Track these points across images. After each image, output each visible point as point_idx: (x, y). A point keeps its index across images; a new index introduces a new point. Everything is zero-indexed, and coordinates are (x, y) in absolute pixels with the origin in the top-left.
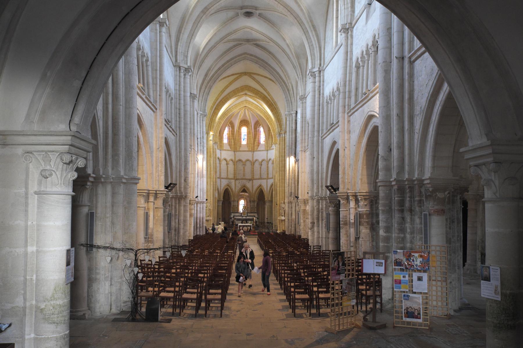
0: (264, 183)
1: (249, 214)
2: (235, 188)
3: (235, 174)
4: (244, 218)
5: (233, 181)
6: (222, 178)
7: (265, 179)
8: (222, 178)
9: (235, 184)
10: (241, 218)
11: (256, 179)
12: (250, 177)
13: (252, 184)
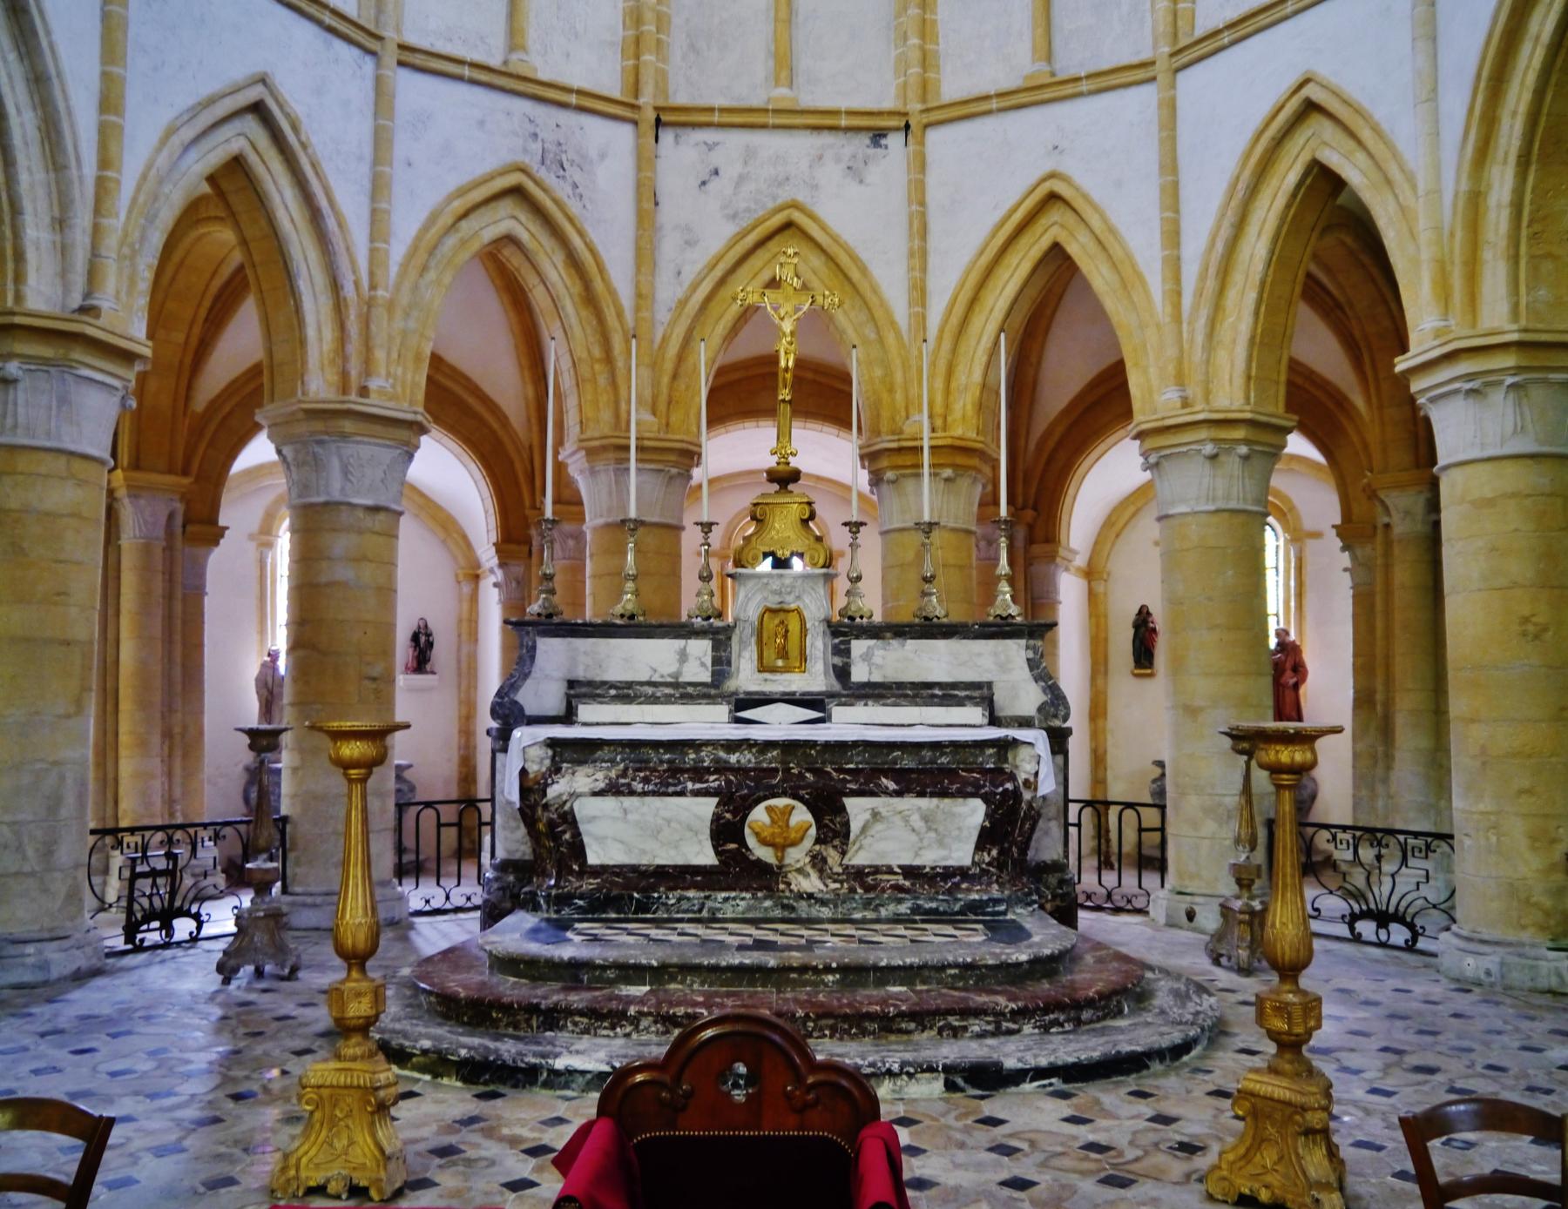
0: (1102, 151)
1: (873, 661)
2: (645, 255)
3: (641, 36)
4: (779, 723)
5: (611, 142)
6: (414, 59)
7: (1135, 74)
8: (414, 59)
9: (647, 199)
10: (706, 722)
11: (972, 109)
12: (877, 90)
13: (918, 193)
